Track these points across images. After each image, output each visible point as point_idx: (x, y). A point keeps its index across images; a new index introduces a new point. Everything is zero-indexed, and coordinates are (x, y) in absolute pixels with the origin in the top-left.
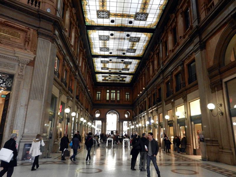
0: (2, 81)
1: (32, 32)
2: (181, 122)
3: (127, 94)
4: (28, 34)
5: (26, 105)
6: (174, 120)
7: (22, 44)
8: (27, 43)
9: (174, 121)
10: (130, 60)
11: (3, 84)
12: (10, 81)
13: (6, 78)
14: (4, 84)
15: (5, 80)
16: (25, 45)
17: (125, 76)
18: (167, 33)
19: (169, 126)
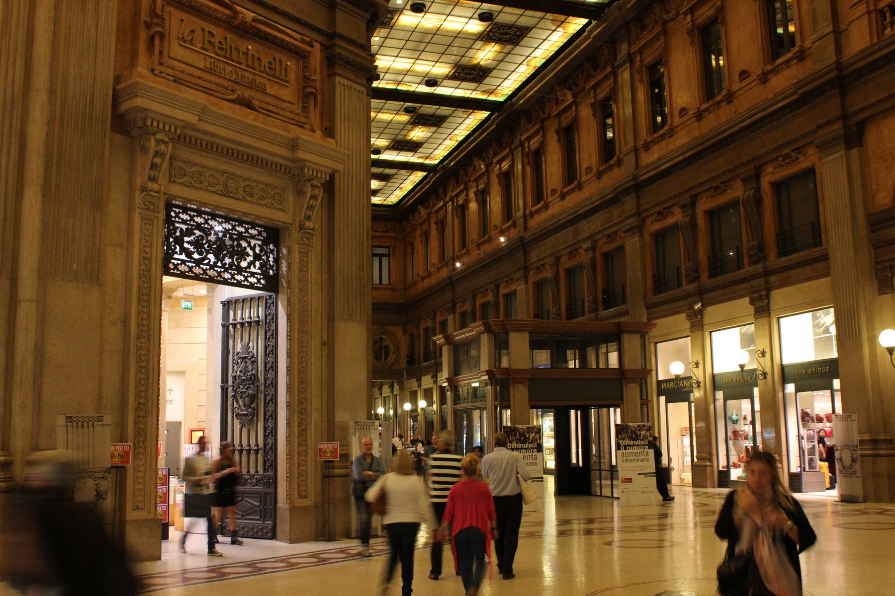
0: (251, 253)
1: (316, 53)
2: (739, 385)
3: (381, 256)
4: (312, 66)
5: (323, 343)
6: (701, 379)
7: (297, 108)
8: (312, 99)
9: (698, 383)
10: (444, 110)
11: (255, 267)
12: (272, 251)
13: (260, 243)
14: (257, 264)
15: (257, 250)
16: (305, 109)
17: (388, 171)
18: (665, 32)
19: (662, 399)
